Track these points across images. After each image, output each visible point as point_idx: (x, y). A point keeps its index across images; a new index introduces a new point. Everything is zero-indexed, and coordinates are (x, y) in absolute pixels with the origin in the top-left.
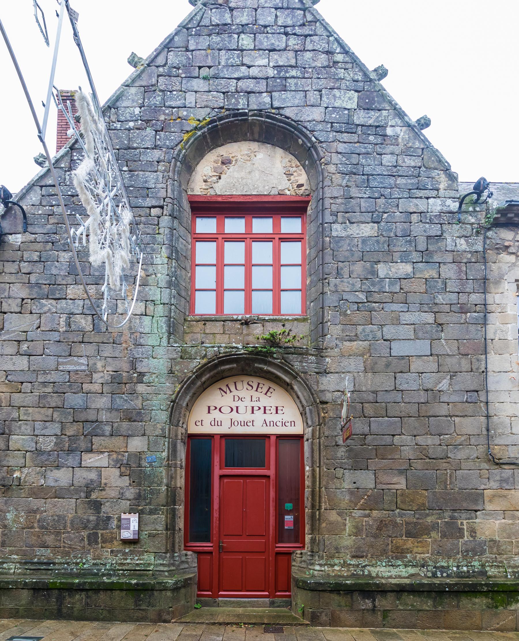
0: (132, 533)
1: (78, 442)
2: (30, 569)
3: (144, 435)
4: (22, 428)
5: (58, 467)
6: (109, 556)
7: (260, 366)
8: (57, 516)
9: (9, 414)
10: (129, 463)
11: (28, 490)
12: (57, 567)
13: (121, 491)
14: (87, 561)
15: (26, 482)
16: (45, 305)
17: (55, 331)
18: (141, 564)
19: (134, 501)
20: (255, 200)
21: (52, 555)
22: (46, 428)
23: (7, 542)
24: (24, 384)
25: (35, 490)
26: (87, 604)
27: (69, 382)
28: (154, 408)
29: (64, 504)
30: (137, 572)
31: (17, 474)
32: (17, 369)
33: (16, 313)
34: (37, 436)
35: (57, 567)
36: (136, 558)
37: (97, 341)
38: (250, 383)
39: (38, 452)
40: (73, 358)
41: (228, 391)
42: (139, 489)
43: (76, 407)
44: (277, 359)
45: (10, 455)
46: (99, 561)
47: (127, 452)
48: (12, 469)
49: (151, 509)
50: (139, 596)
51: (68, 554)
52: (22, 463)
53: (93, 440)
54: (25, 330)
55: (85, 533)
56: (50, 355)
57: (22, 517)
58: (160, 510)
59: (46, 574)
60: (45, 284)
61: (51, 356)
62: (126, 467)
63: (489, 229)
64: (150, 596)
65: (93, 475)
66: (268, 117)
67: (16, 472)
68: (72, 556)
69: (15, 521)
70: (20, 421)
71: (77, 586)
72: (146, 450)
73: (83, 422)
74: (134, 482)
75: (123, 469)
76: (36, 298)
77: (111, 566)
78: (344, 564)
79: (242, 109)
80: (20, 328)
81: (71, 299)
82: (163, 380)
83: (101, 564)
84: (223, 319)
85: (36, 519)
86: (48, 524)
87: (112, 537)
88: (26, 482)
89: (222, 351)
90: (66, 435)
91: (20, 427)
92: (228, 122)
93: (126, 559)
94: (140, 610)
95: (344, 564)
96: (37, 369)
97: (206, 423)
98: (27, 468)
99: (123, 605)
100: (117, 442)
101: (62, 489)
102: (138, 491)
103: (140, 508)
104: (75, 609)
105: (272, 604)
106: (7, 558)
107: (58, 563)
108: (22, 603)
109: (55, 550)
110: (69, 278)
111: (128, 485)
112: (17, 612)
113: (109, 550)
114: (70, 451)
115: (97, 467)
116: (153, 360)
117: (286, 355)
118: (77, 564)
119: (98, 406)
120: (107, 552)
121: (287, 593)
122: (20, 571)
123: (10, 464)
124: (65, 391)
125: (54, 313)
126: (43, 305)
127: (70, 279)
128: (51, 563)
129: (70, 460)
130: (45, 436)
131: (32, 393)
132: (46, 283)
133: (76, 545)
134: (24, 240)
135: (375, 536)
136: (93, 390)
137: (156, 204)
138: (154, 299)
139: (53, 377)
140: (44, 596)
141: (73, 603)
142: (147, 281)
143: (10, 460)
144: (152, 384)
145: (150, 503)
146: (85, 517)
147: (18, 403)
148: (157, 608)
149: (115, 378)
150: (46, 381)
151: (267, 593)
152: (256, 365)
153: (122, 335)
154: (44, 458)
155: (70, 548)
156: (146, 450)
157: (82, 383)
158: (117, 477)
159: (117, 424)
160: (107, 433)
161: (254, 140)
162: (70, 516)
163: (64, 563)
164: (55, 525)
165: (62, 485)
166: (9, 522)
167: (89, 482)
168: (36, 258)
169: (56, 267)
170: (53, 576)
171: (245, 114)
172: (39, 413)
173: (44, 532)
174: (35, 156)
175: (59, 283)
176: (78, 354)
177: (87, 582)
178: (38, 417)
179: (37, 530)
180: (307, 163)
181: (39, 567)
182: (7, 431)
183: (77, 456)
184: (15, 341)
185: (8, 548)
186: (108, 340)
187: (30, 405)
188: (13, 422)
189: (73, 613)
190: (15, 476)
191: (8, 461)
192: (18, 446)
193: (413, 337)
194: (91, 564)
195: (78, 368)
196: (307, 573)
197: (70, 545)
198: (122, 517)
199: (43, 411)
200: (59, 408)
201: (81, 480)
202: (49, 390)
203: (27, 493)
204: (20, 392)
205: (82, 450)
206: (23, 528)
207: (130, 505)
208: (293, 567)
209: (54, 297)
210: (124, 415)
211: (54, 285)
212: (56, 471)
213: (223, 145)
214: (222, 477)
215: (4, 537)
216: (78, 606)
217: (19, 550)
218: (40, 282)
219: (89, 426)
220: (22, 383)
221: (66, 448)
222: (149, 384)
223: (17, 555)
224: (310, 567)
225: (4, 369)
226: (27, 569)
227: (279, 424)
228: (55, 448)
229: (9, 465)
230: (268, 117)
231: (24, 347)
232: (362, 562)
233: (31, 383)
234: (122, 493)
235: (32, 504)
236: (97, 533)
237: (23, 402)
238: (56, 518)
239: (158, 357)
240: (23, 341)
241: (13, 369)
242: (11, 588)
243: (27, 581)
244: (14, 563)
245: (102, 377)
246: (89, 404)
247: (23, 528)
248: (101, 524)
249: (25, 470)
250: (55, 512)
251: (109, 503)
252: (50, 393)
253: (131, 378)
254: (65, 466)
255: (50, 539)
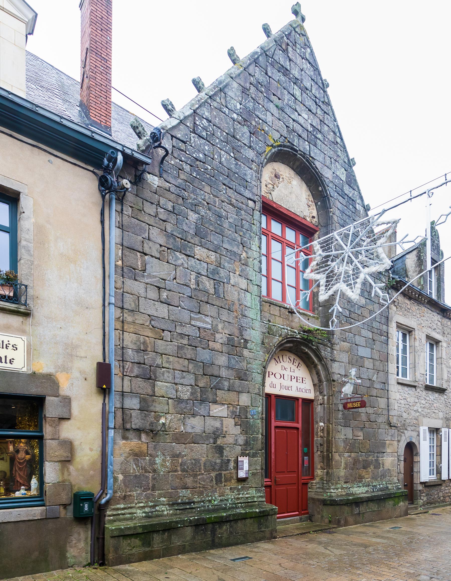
0: (245, 472)
1: (207, 393)
2: (180, 510)
3: (248, 392)
4: (165, 375)
5: (194, 415)
6: (229, 493)
7: (305, 348)
8: (194, 460)
9: (154, 360)
10: (240, 415)
11: (172, 436)
12: (196, 505)
13: (236, 438)
14: (215, 498)
15: (170, 428)
16: (179, 259)
17: (187, 286)
18: (249, 497)
19: (244, 447)
20: (292, 216)
21: (191, 495)
22: (184, 378)
23: (156, 486)
24: (165, 332)
25: (178, 435)
26: (231, 533)
27: (199, 337)
28: (254, 371)
29: (199, 449)
30: (250, 504)
31: (162, 421)
32: (159, 316)
33: (156, 258)
34: (176, 384)
35: (196, 505)
36: (245, 493)
37: (217, 305)
38: (290, 358)
39: (179, 400)
40: (201, 315)
41: (279, 362)
42: (247, 437)
43: (204, 362)
44: (314, 346)
45: (157, 400)
46: (223, 497)
47: (239, 405)
48: (159, 415)
49: (253, 453)
50: (260, 521)
51: (201, 493)
52: (167, 410)
53: (217, 393)
54: (164, 278)
55: (213, 474)
56: (184, 309)
57: (168, 461)
58: (259, 453)
59: (192, 512)
60: (178, 237)
61: (185, 309)
62: (238, 418)
63: (390, 289)
64: (266, 520)
65: (217, 424)
66: (307, 161)
67: (162, 418)
68: (205, 495)
69: (162, 465)
70: (163, 367)
71: (226, 519)
72: (250, 405)
73: (210, 376)
74: (243, 430)
75: (237, 419)
76: (171, 249)
77: (231, 501)
78: (342, 488)
79: (296, 146)
80: (160, 275)
81: (198, 259)
82: (258, 349)
83: (226, 500)
84: (280, 305)
85: (178, 463)
86: (188, 467)
87: (231, 477)
88: (170, 428)
89: (289, 334)
90: (198, 386)
91: (163, 374)
92: (287, 151)
93: (239, 494)
94: (261, 531)
95: (342, 488)
96: (175, 319)
97: (294, 388)
98: (170, 415)
99: (252, 529)
100: (232, 396)
101: (197, 435)
102: (246, 438)
103: (247, 452)
104: (223, 538)
105: (301, 520)
106: (157, 501)
107: (196, 502)
108: (187, 539)
109: (193, 491)
110: (196, 239)
111: (240, 433)
112: (184, 548)
113: (229, 487)
114: (203, 401)
115: (220, 417)
116: (252, 331)
117: (318, 345)
118: (210, 501)
119: (220, 364)
120: (228, 489)
121: (306, 511)
122: (171, 512)
123: (157, 409)
124: (197, 345)
125: (186, 268)
126: (177, 259)
127: (196, 240)
128: (191, 503)
129: (202, 409)
130: (183, 385)
131: (171, 341)
132: (179, 236)
133: (208, 485)
134: (160, 185)
135: (353, 469)
136: (216, 348)
137: (252, 198)
138: (252, 279)
139: (187, 330)
140: (203, 530)
141: (222, 534)
142: (247, 262)
143: (157, 405)
144: (253, 351)
145: (252, 449)
146: (213, 460)
147: (161, 350)
148: (270, 529)
149: (230, 341)
150: (182, 333)
151: (297, 513)
152: (302, 347)
153: (234, 304)
154: (183, 405)
155: (204, 488)
156: (250, 405)
157: (208, 341)
158: (233, 426)
159: (232, 380)
160: (226, 389)
161: (292, 169)
162: (203, 459)
163: (201, 502)
164: (193, 467)
165: (197, 432)
166: (158, 467)
167: (215, 429)
168: (170, 208)
169: (186, 223)
170: (197, 514)
171: (296, 151)
172: (178, 362)
173: (185, 474)
174: (164, 99)
175: (188, 240)
176: (206, 313)
177: (231, 514)
178: (177, 367)
179: (179, 473)
180: (319, 203)
181: (185, 507)
182: (153, 377)
183: (207, 406)
184: (156, 286)
185: (157, 492)
186: (225, 306)
187: (171, 354)
188: (157, 368)
189: (222, 541)
190: (161, 422)
191: (155, 407)
192: (162, 392)
193: (365, 346)
194: (219, 500)
195: (204, 326)
196: (325, 495)
197: (204, 485)
198: (239, 460)
199: (181, 360)
200: (193, 360)
201: (210, 427)
202: (185, 342)
203: (171, 438)
204: (162, 339)
205: (210, 401)
206: (169, 472)
207: (241, 450)
208: (309, 493)
209: (186, 253)
210: (236, 374)
211: (185, 241)
212: (192, 419)
213: (276, 162)
214: (276, 427)
215: (154, 481)
216: (225, 535)
217: (166, 492)
218: (175, 234)
219: (214, 380)
220: (163, 330)
221: (199, 398)
222: (250, 350)
223: (165, 498)
224: (327, 491)
225: (148, 313)
226: (177, 510)
227: (304, 391)
228: (191, 397)
229: (156, 411)
230: (307, 161)
231: (164, 295)
232: (348, 485)
233: (170, 332)
234: (237, 440)
235: (176, 449)
236: (221, 474)
237: (165, 349)
238: (193, 461)
239: (256, 329)
240: (163, 288)
241: (156, 315)
242: (180, 527)
243: (191, 519)
244: (165, 505)
245: (221, 338)
246: (214, 361)
247: (169, 472)
248: (224, 466)
249: (168, 416)
250: (192, 456)
251: (228, 448)
252: (185, 345)
253: (240, 343)
254: (199, 414)
255: (189, 481)
